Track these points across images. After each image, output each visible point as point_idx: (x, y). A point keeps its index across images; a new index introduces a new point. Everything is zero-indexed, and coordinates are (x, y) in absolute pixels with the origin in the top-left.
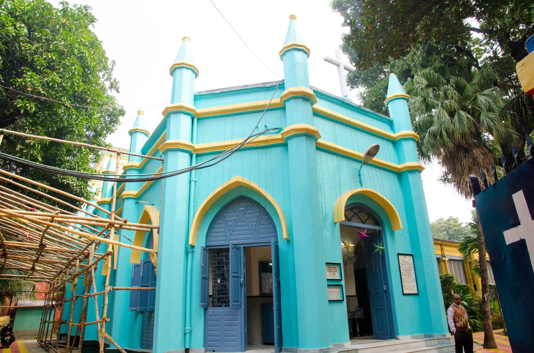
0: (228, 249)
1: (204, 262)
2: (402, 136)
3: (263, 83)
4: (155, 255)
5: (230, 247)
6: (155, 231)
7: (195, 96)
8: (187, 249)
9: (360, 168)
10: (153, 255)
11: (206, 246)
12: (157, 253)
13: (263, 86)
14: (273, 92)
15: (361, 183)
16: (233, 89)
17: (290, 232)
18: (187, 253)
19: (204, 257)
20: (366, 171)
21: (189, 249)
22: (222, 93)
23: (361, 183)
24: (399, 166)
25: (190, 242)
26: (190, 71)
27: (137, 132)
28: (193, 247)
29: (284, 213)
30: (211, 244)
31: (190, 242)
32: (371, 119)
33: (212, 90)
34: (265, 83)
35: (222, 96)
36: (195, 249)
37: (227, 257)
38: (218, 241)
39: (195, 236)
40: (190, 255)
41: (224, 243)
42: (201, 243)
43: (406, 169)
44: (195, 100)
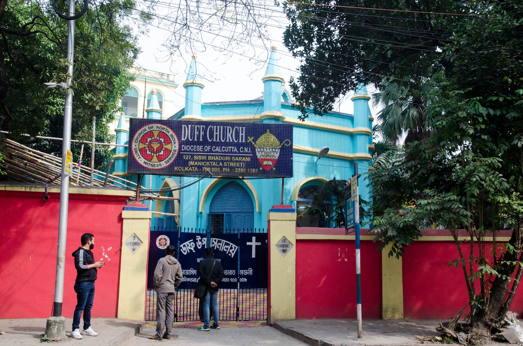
0: (223, 215)
1: (208, 223)
2: (357, 132)
3: (250, 101)
4: (178, 217)
5: (225, 214)
6: (176, 202)
7: (202, 105)
8: (197, 214)
9: (317, 161)
10: (176, 217)
11: (210, 213)
12: (179, 216)
13: (249, 103)
14: (257, 108)
15: (316, 171)
16: (229, 104)
17: (260, 208)
18: (198, 217)
19: (208, 220)
20: (323, 161)
21: (199, 215)
22: (221, 105)
23: (316, 171)
24: (351, 155)
25: (200, 211)
26: (198, 88)
27: (153, 111)
28: (201, 213)
29: (257, 196)
30: (213, 211)
31: (200, 211)
32: (335, 118)
33: (214, 103)
34: (252, 101)
35: (221, 108)
36: (203, 214)
37: (223, 219)
38: (218, 210)
39: (203, 207)
40: (199, 218)
41: (221, 211)
42: (206, 211)
43: (356, 159)
44: (202, 108)
